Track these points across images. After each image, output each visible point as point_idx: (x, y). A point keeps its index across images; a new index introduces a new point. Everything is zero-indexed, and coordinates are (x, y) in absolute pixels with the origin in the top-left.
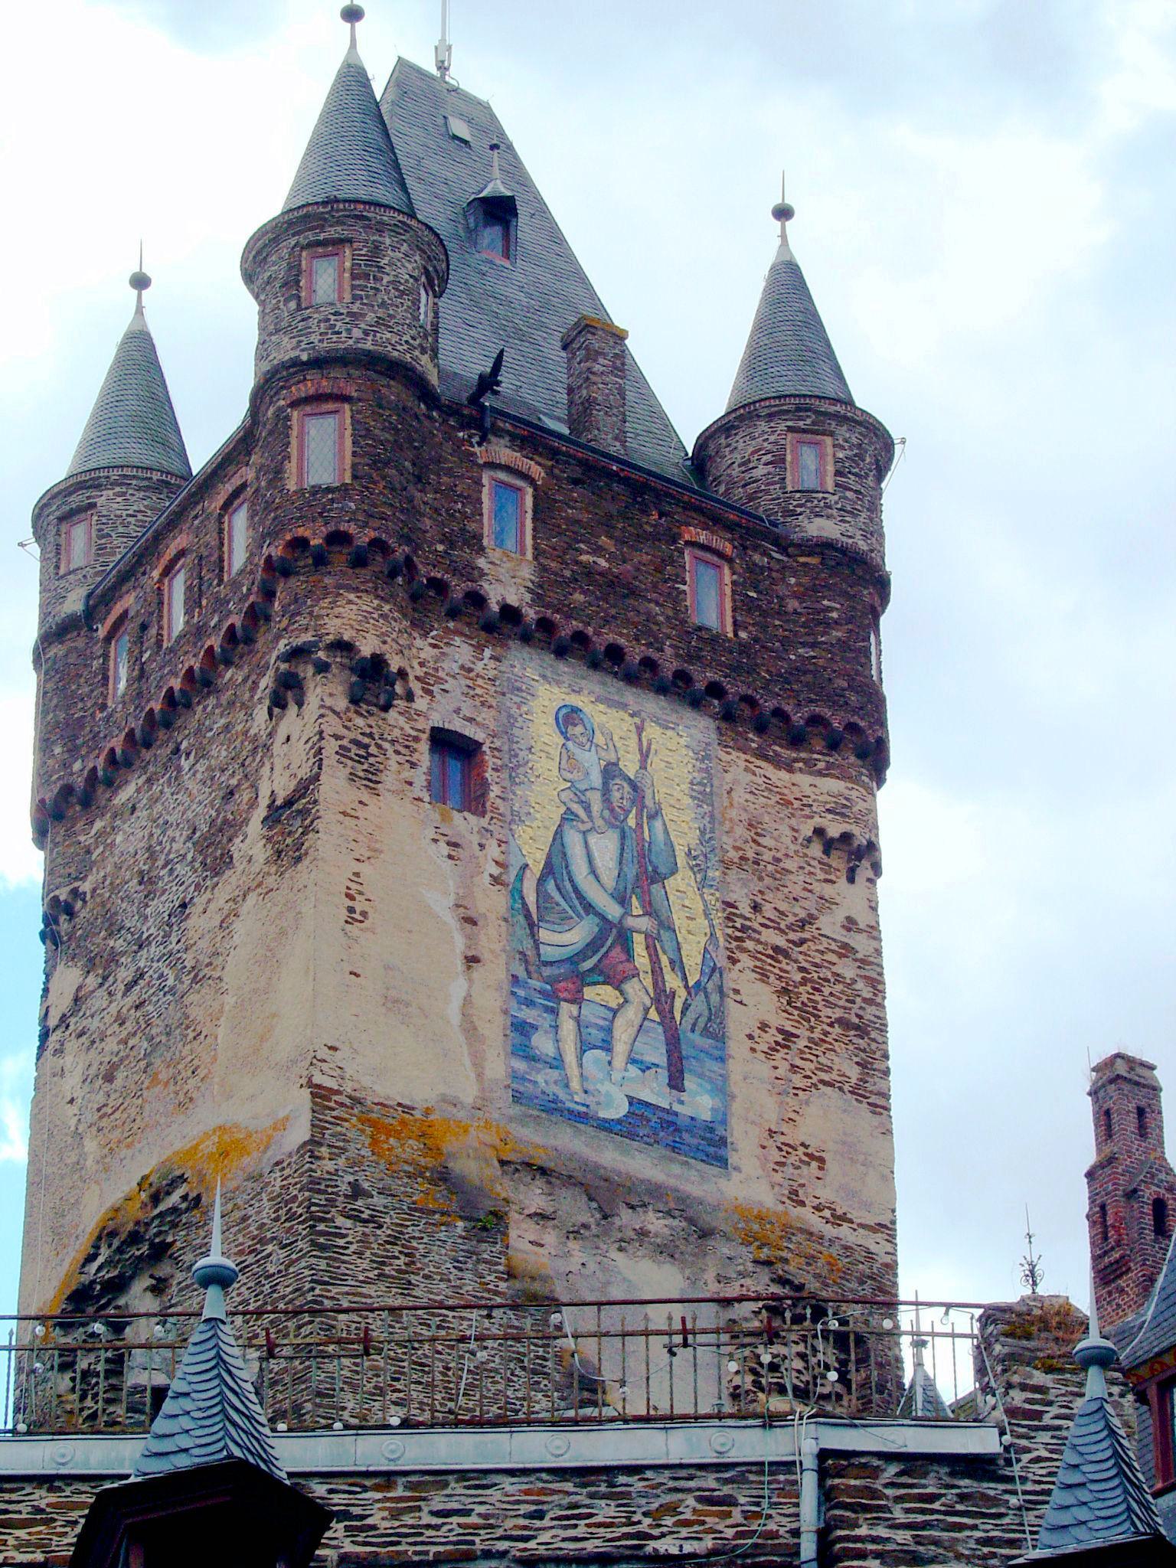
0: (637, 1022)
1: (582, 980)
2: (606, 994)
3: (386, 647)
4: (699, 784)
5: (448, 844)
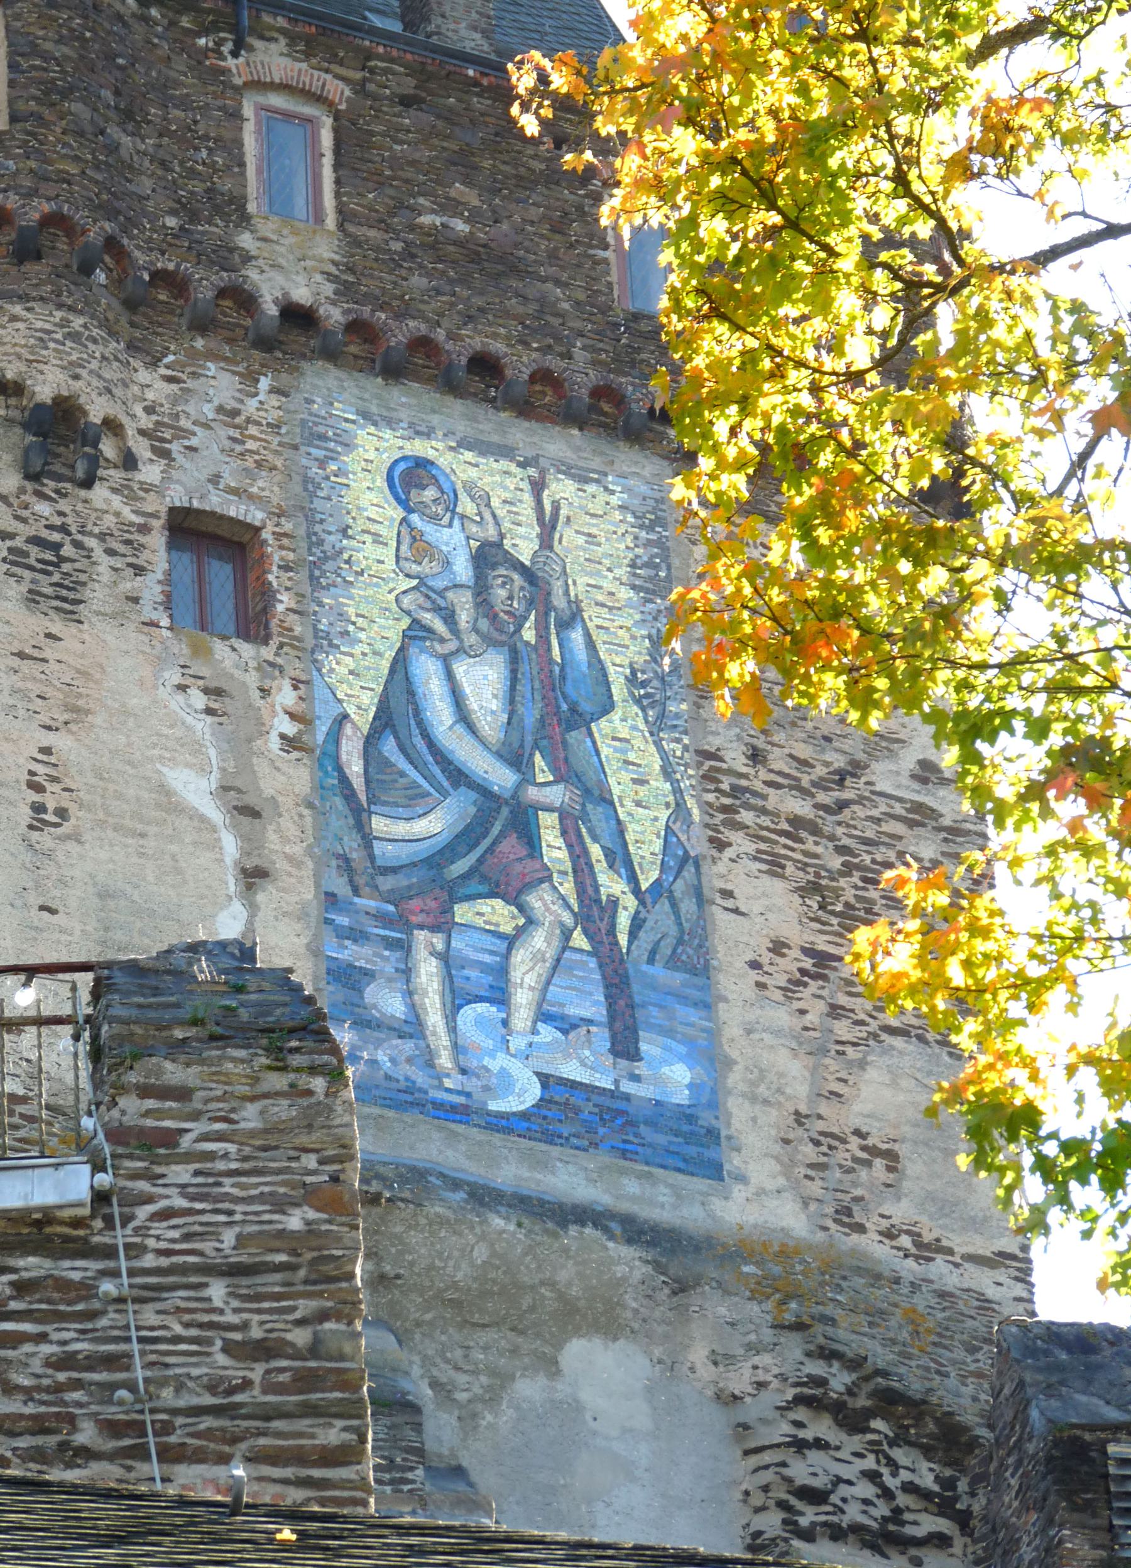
0: (550, 954)
1: (454, 893)
3: (80, 384)
4: (648, 565)
5: (206, 691)
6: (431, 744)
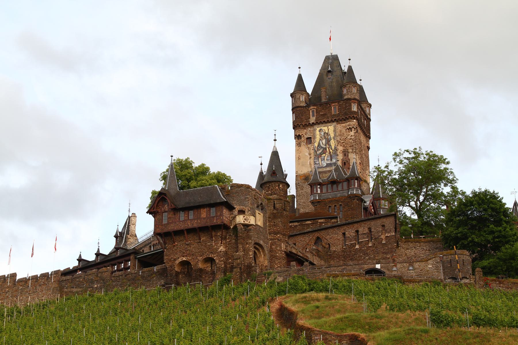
1: (322, 155)
2: (324, 155)
6: (321, 146)
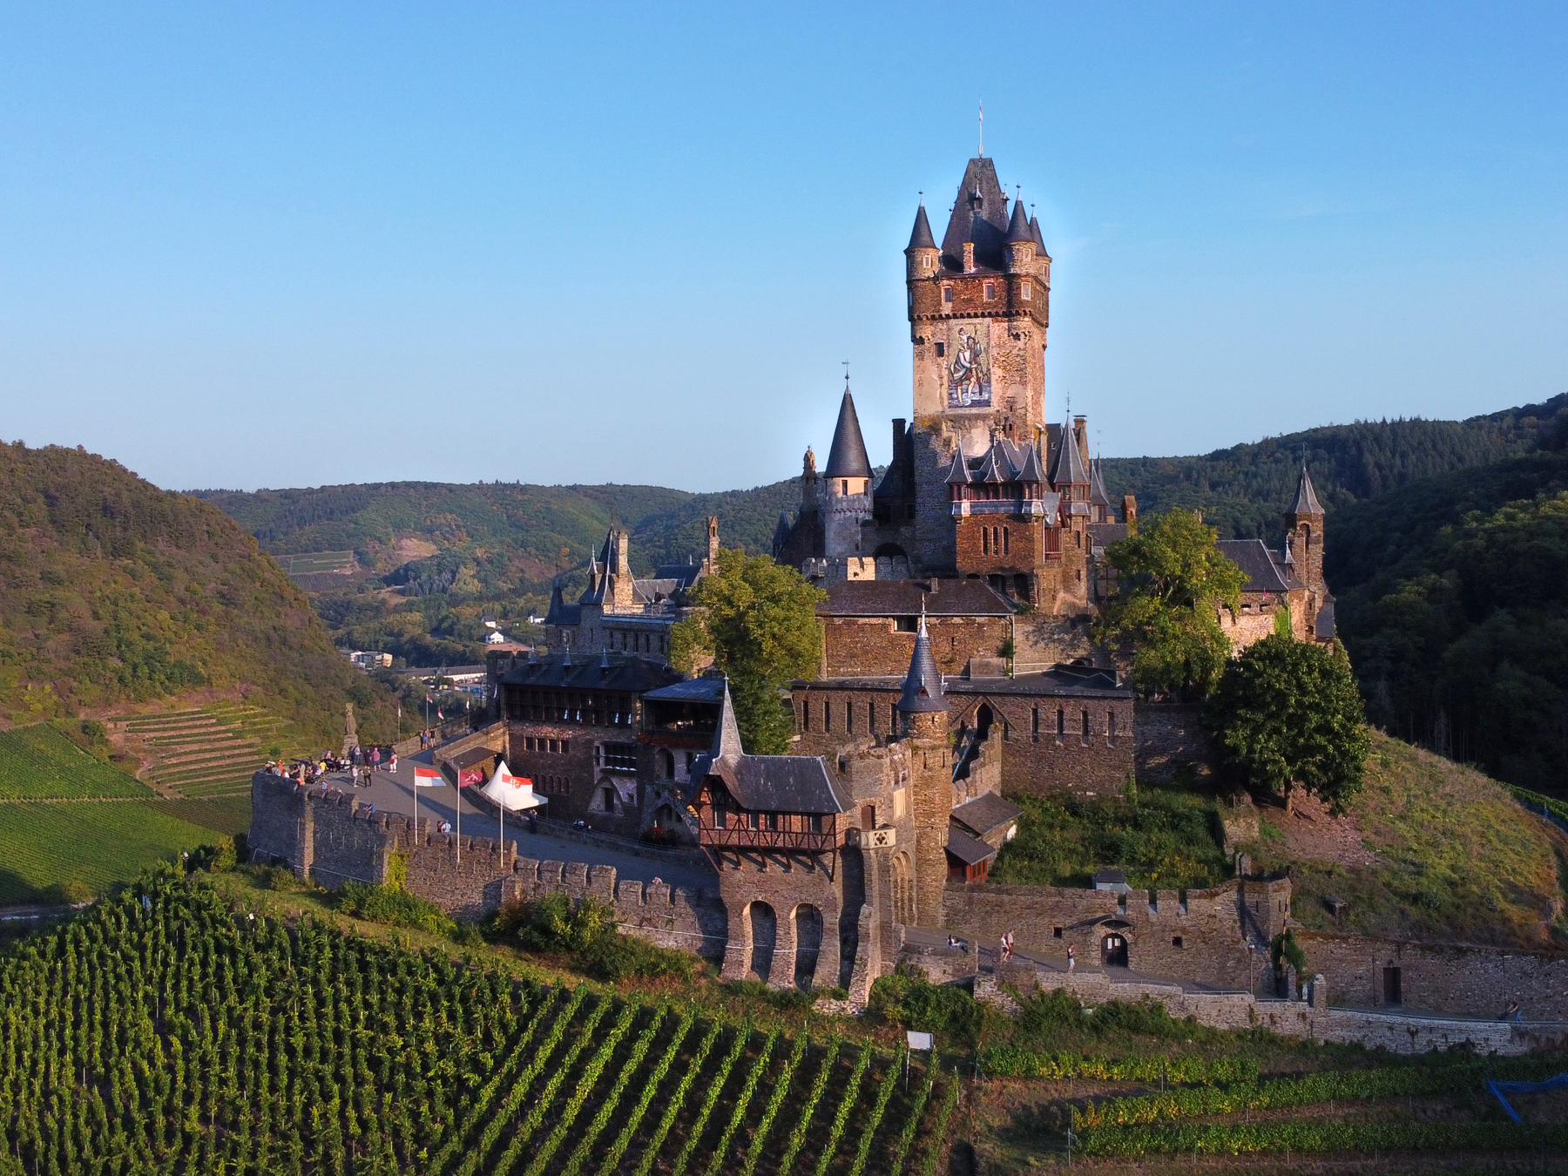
2: (967, 382)
